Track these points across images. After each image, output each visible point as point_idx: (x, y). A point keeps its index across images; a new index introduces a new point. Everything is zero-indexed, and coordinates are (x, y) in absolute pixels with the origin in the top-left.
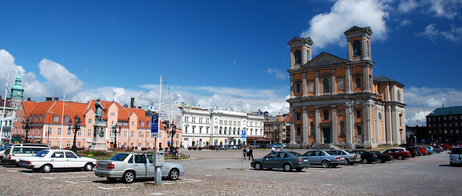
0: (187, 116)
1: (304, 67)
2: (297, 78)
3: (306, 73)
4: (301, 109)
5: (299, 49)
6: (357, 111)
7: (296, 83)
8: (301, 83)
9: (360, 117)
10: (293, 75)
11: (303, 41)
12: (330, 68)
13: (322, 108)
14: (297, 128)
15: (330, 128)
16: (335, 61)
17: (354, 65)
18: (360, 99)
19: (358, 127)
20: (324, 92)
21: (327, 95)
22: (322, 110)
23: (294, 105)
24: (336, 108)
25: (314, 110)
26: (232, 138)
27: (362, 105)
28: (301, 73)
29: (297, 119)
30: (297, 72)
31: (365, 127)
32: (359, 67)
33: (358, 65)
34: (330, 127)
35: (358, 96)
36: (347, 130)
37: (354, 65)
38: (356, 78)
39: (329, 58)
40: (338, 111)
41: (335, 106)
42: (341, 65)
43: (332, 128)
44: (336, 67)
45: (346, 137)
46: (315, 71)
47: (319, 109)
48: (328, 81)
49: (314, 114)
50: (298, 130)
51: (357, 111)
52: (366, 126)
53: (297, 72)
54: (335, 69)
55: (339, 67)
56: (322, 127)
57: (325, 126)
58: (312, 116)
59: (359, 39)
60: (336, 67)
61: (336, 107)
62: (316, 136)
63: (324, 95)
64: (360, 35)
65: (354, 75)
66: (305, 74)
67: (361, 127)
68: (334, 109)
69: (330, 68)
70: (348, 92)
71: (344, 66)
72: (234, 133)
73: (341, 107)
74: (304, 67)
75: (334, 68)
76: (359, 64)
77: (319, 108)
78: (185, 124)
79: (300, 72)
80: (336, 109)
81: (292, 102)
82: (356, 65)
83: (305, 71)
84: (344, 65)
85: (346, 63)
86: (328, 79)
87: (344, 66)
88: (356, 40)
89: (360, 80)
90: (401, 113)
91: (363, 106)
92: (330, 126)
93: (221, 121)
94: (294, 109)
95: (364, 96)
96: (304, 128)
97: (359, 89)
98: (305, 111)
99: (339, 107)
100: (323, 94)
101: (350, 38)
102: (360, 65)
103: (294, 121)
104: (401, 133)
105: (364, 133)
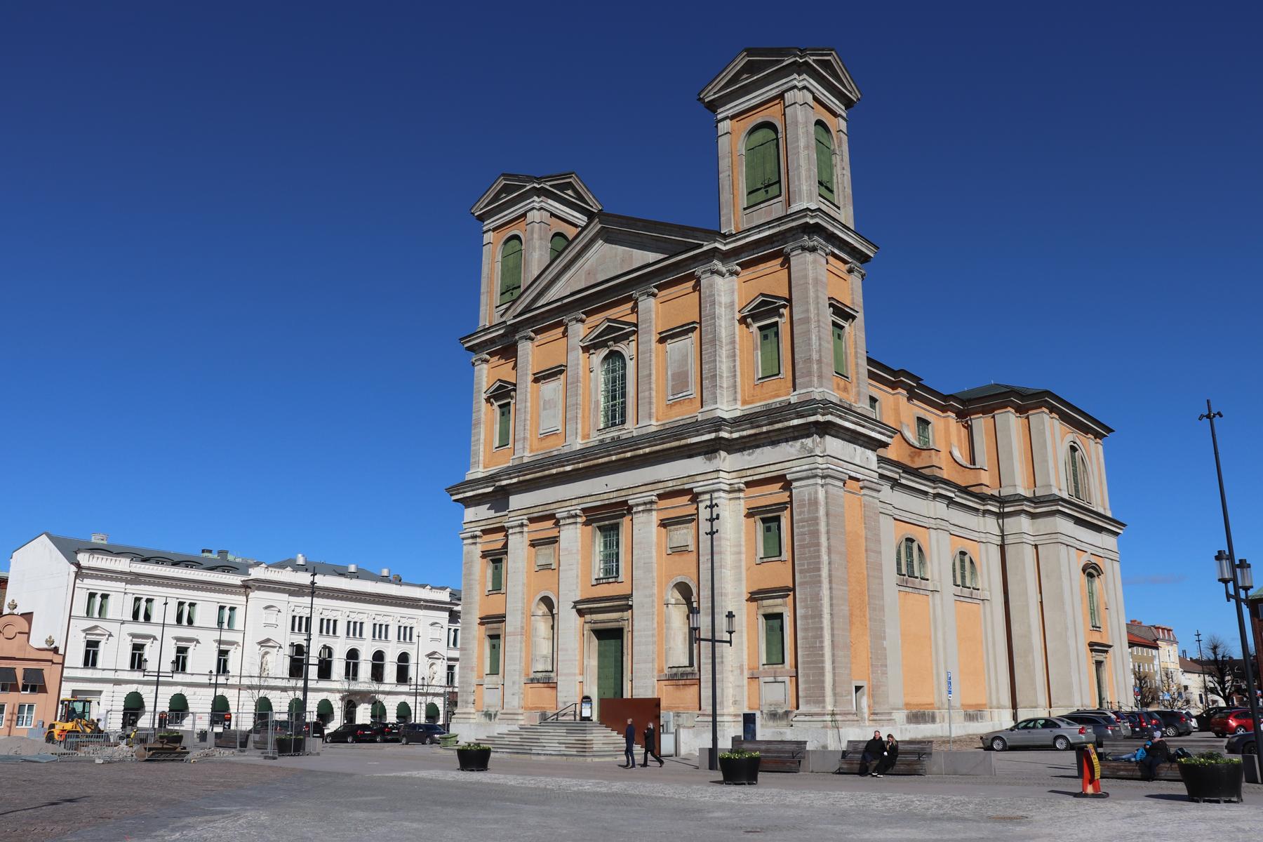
0: (99, 586)
1: (519, 310)
5: (516, 232)
6: (764, 520)
21: (613, 438)
25: (554, 533)
26: (366, 696)
31: (805, 617)
52: (806, 607)
64: (774, 93)
72: (377, 674)
78: (89, 623)
85: (701, 246)
88: (760, 120)
90: (1094, 560)
93: (301, 624)
97: (772, 384)
104: (1099, 664)
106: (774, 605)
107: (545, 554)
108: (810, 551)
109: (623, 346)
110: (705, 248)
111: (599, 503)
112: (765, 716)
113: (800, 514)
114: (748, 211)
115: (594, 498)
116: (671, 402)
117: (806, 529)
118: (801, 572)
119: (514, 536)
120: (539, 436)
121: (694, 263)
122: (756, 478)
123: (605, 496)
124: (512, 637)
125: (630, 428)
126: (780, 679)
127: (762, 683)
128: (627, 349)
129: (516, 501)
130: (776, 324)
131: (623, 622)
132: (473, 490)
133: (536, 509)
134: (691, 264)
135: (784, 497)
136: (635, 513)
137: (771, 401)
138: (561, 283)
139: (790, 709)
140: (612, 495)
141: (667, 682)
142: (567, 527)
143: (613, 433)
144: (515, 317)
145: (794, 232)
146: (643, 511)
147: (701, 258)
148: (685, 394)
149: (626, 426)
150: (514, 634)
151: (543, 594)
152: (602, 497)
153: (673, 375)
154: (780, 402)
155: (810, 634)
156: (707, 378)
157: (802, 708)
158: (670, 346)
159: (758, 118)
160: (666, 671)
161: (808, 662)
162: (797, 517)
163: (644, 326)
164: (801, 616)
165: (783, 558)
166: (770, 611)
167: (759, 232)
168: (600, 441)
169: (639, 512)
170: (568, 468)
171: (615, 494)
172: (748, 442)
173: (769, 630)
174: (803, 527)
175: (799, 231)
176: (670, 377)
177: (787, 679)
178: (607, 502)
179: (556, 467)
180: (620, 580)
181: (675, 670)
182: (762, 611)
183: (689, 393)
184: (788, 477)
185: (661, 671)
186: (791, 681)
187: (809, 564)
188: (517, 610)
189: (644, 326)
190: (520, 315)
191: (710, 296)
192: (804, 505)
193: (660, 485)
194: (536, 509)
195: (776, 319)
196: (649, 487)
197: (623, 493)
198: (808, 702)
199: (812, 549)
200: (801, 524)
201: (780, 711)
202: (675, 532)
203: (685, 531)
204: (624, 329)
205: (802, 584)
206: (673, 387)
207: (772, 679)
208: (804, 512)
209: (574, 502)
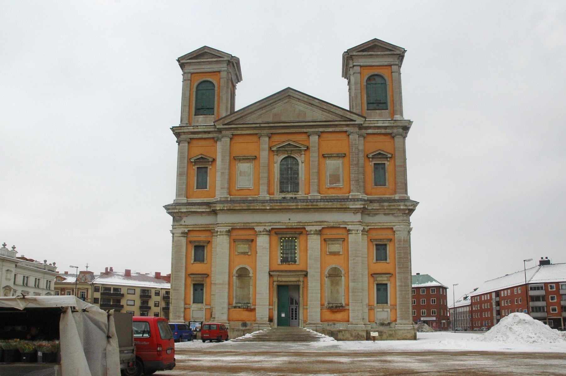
1: (226, 122)
2: (198, 150)
3: (231, 139)
4: (208, 234)
6: (376, 245)
7: (196, 162)
8: (211, 165)
9: (386, 260)
10: (189, 143)
11: (225, 59)
12: (305, 130)
13: (276, 233)
14: (194, 285)
15: (298, 286)
16: (319, 115)
17: (370, 131)
18: (385, 214)
19: (377, 285)
20: (282, 191)
21: (292, 198)
22: (275, 238)
23: (190, 221)
24: (319, 232)
27: (392, 228)
28: (213, 138)
29: (195, 261)
30: (200, 136)
31: (401, 286)
32: (383, 137)
33: (383, 131)
34: (301, 283)
35: (383, 206)
36: (350, 291)
37: (370, 131)
38: (375, 164)
39: (301, 107)
40: (323, 242)
41: (319, 228)
42: (336, 126)
43: (306, 287)
44: (321, 130)
45: (349, 309)
46: (259, 136)
47: (269, 232)
48: (297, 164)
49: (250, 248)
50: (195, 290)
51: (376, 245)
53: (200, 136)
54: (320, 135)
55: (330, 130)
56: (275, 283)
57: (284, 279)
58: (245, 253)
59: (384, 72)
60: (321, 130)
61: (320, 231)
62: (255, 305)
63: (284, 198)
64: (386, 63)
65: (370, 156)
66: (228, 140)
67: (387, 284)
68: (315, 237)
69: (305, 130)
70: (356, 194)
71: (345, 129)
73: (334, 231)
74: (230, 120)
75: (316, 130)
76: (385, 127)
77: (270, 231)
79: (211, 136)
80: (319, 237)
81: (183, 210)
82: (376, 131)
83: (229, 133)
84: (347, 125)
85: (355, 121)
86: (298, 159)
87: (345, 129)
88: (376, 73)
89: (384, 168)
91: (394, 232)
92: (299, 281)
94: (186, 230)
95: (400, 206)
96: (219, 284)
97: (381, 189)
98: (225, 237)
99: (328, 232)
100: (278, 196)
101: (361, 66)
102: (388, 131)
103: (184, 265)
105: (398, 300)
106: (383, 279)
107: (243, 247)
108: (404, 260)
109: (297, 155)
110: (356, 123)
111: (285, 227)
112: (378, 324)
113: (399, 244)
114: (369, 111)
115: (281, 224)
116: (328, 187)
117: (402, 251)
118: (399, 268)
119: (221, 236)
120: (237, 189)
121: (346, 127)
122: (375, 227)
123: (290, 224)
124: (221, 286)
125: (301, 195)
126: (385, 310)
127: (375, 312)
128: (300, 159)
129: (222, 218)
130: (207, 167)
131: (299, 283)
132: (187, 209)
133: (239, 225)
134: (344, 127)
135: (391, 237)
136: (309, 234)
137: (382, 196)
138: (255, 115)
139: (390, 322)
140: (294, 225)
141: (327, 310)
142: (261, 236)
143: (289, 196)
144: (223, 125)
145: (398, 128)
146: (314, 234)
147: (351, 126)
148: (337, 185)
149: (300, 193)
150: (222, 284)
151: (241, 266)
152: (286, 225)
153: (330, 175)
154: (387, 198)
155: (403, 293)
156: (353, 180)
157: (398, 321)
158: (329, 162)
159: (376, 72)
160: (326, 306)
161: (402, 304)
162: (397, 246)
163: (313, 149)
164: (399, 285)
165: (388, 261)
166: (381, 282)
167: (383, 123)
168: (283, 198)
169: (312, 234)
170: (268, 208)
171: (296, 224)
172: (372, 212)
173: (378, 290)
174: (400, 250)
175: (401, 128)
176: (328, 175)
177: (389, 310)
178: (290, 227)
179: (259, 206)
180: (297, 263)
181: (331, 305)
182: (376, 282)
183: (339, 185)
184: (394, 229)
185: (322, 305)
186: (391, 311)
187: (403, 265)
188: (225, 273)
189: (313, 149)
190: (226, 124)
191: (355, 144)
192: (401, 241)
193: (325, 224)
194: (239, 225)
195: (385, 162)
196: (318, 224)
197: (301, 224)
198: (401, 319)
199: (405, 259)
200: (399, 249)
201: (386, 322)
202: (332, 245)
203: (338, 245)
204: (301, 148)
205: (398, 273)
206: (330, 181)
207: (381, 310)
208: (401, 244)
209: (267, 224)
